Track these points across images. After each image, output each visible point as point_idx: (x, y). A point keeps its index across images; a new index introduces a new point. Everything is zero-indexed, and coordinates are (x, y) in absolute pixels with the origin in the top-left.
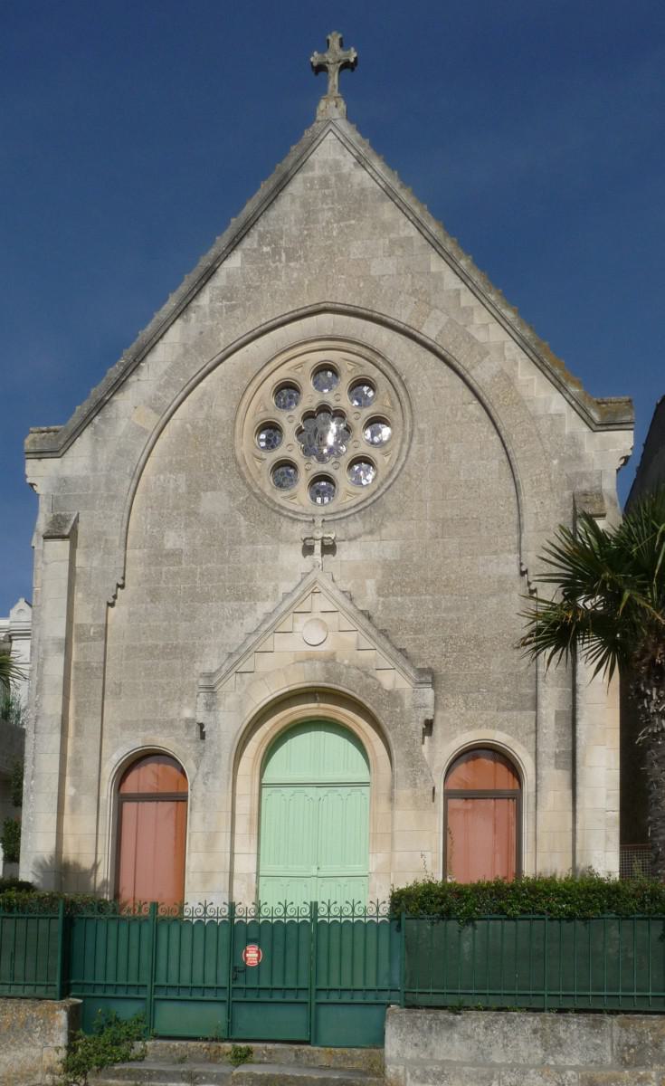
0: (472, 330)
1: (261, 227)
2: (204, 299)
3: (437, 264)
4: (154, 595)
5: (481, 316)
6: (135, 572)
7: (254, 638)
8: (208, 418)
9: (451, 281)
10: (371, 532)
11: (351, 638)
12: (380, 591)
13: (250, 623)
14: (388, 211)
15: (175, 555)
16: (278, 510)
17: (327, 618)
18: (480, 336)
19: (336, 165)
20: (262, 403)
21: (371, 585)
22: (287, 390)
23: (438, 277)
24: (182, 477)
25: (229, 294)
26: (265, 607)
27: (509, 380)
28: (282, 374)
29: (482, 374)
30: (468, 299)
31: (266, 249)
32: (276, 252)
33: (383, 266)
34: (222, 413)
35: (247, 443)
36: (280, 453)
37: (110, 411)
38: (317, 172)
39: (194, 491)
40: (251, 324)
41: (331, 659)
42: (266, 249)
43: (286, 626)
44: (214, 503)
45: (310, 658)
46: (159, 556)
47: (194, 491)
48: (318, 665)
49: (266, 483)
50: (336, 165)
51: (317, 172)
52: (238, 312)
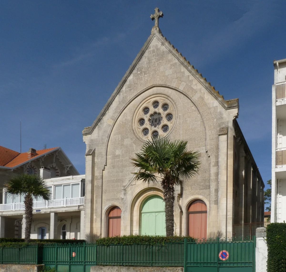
0: (192, 86)
2: (124, 88)
3: (183, 69)
4: (114, 167)
5: (195, 82)
8: (126, 120)
9: (187, 73)
14: (170, 56)
15: (118, 156)
19: (157, 45)
23: (184, 73)
25: (130, 86)
30: (191, 78)
31: (139, 72)
32: (141, 73)
38: (152, 49)
39: (123, 139)
42: (139, 72)
46: (115, 157)
47: (123, 139)
51: (152, 49)
52: (132, 91)
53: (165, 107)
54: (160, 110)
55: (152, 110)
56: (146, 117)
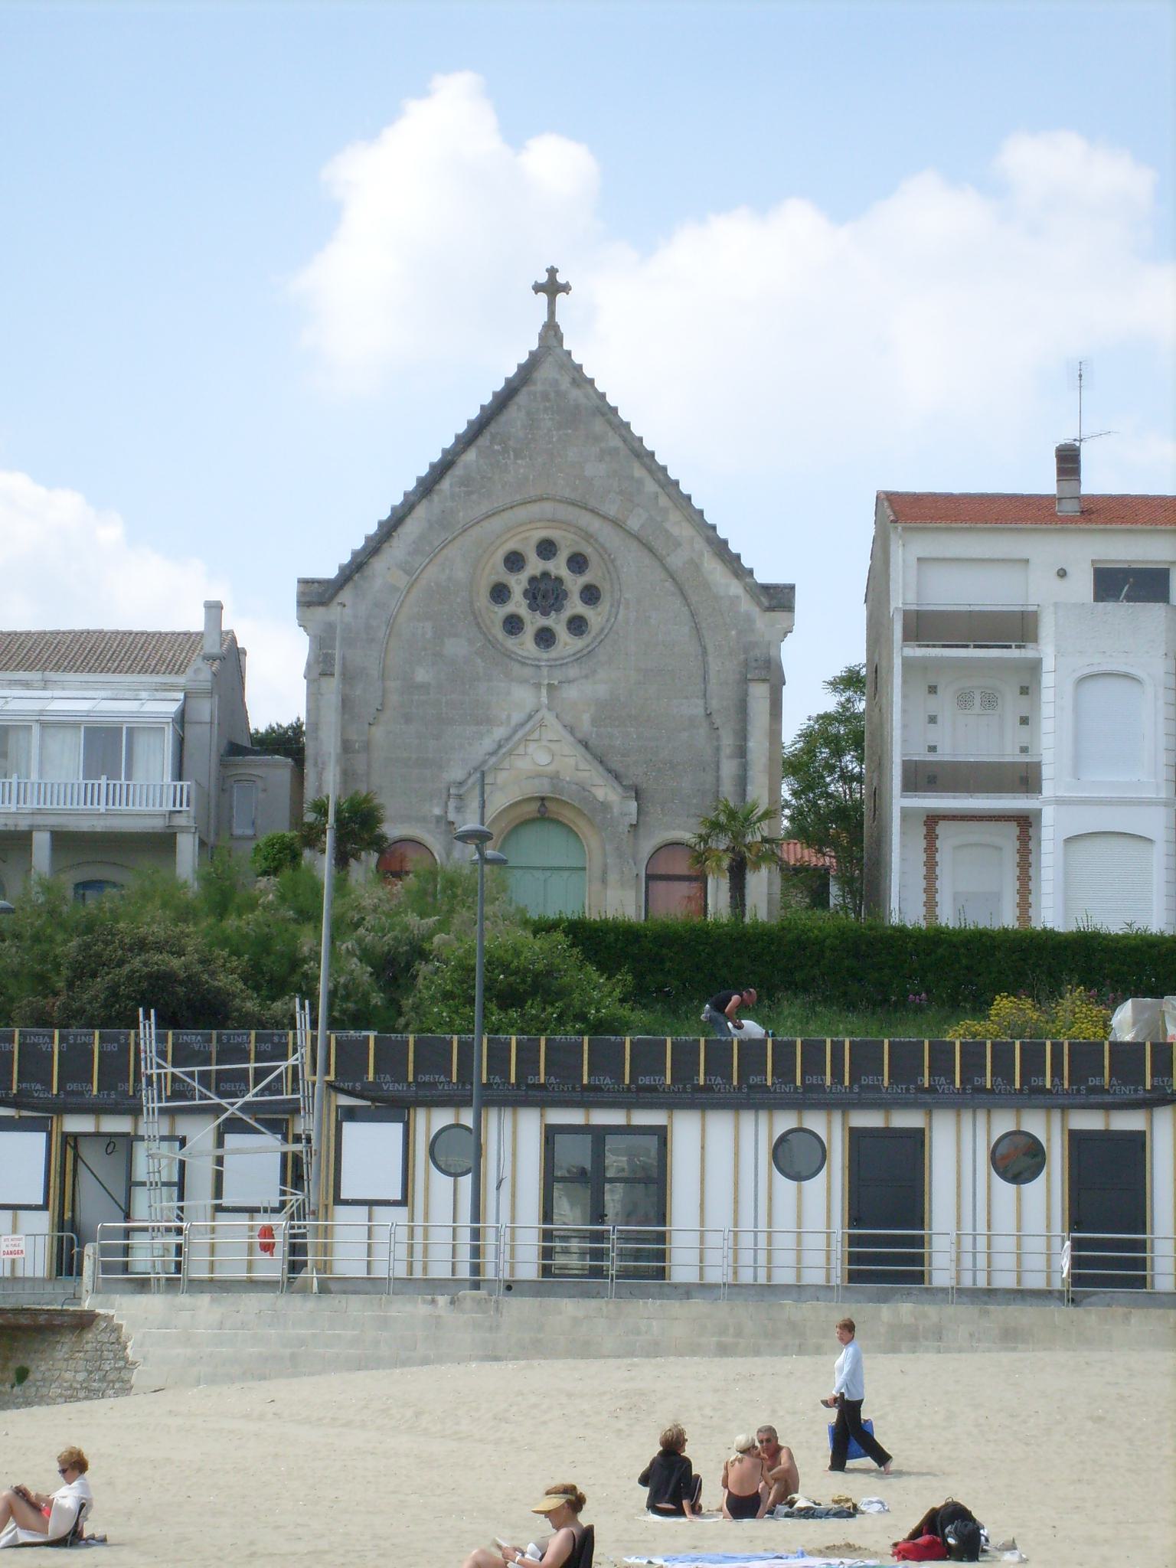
1: (493, 428)
2: (446, 485)
6: (394, 698)
7: (493, 759)
10: (586, 677)
11: (572, 761)
12: (595, 722)
13: (488, 744)
15: (424, 687)
16: (509, 655)
17: (553, 746)
18: (675, 531)
19: (556, 382)
20: (494, 570)
21: (586, 718)
22: (514, 561)
24: (429, 625)
25: (466, 482)
26: (499, 732)
27: (695, 566)
28: (511, 545)
29: (676, 560)
31: (496, 447)
33: (595, 470)
34: (461, 575)
35: (483, 599)
36: (510, 608)
37: (368, 571)
40: (485, 507)
41: (555, 777)
42: (496, 447)
43: (521, 750)
44: (456, 647)
45: (539, 775)
48: (546, 781)
49: (499, 632)
50: (556, 382)
52: (474, 497)
53: (578, 563)
54: (558, 567)
55: (535, 565)
56: (518, 584)
